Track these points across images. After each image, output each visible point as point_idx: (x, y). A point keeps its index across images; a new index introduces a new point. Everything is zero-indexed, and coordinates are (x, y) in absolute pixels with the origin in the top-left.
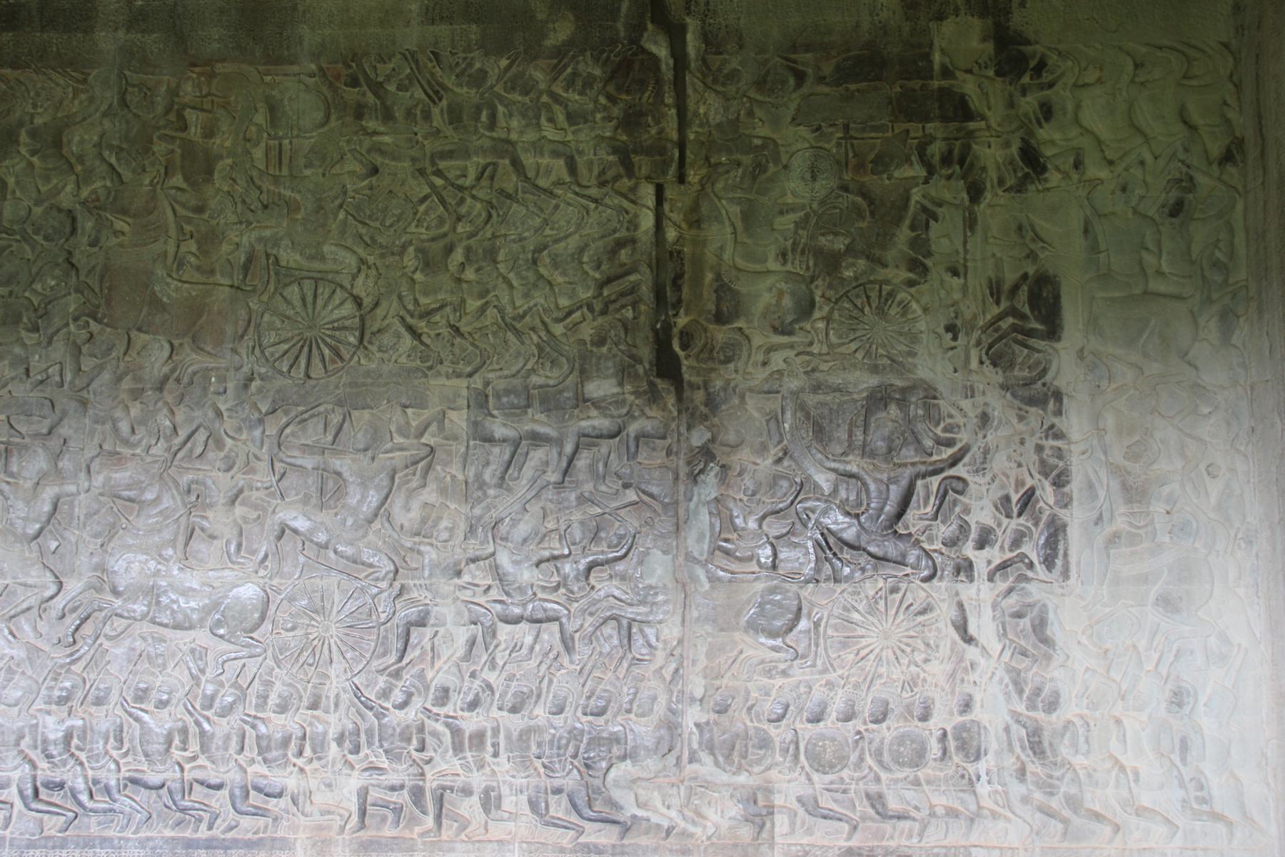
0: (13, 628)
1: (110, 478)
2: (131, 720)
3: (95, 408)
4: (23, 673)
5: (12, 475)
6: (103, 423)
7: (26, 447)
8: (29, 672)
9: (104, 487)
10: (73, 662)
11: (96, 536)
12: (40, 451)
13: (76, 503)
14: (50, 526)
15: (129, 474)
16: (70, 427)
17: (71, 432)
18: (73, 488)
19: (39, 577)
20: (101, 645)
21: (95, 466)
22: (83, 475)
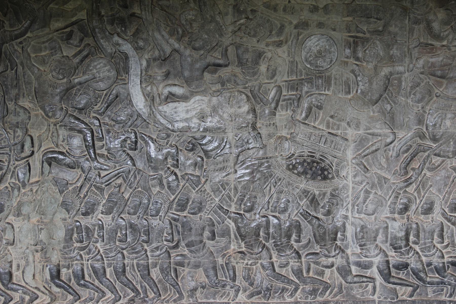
0: (366, 164)
1: (428, 62)
2: (449, 224)
3: (414, 13)
4: (376, 193)
5: (357, 59)
6: (420, 24)
7: (367, 40)
8: (380, 193)
9: (423, 67)
10: (407, 186)
11: (419, 101)
12: (378, 42)
13: (403, 79)
14: (386, 95)
15: (441, 59)
16: (396, 26)
17: (397, 29)
18: (401, 69)
19: (381, 129)
20: (425, 174)
21: (415, 53)
22: (407, 60)
